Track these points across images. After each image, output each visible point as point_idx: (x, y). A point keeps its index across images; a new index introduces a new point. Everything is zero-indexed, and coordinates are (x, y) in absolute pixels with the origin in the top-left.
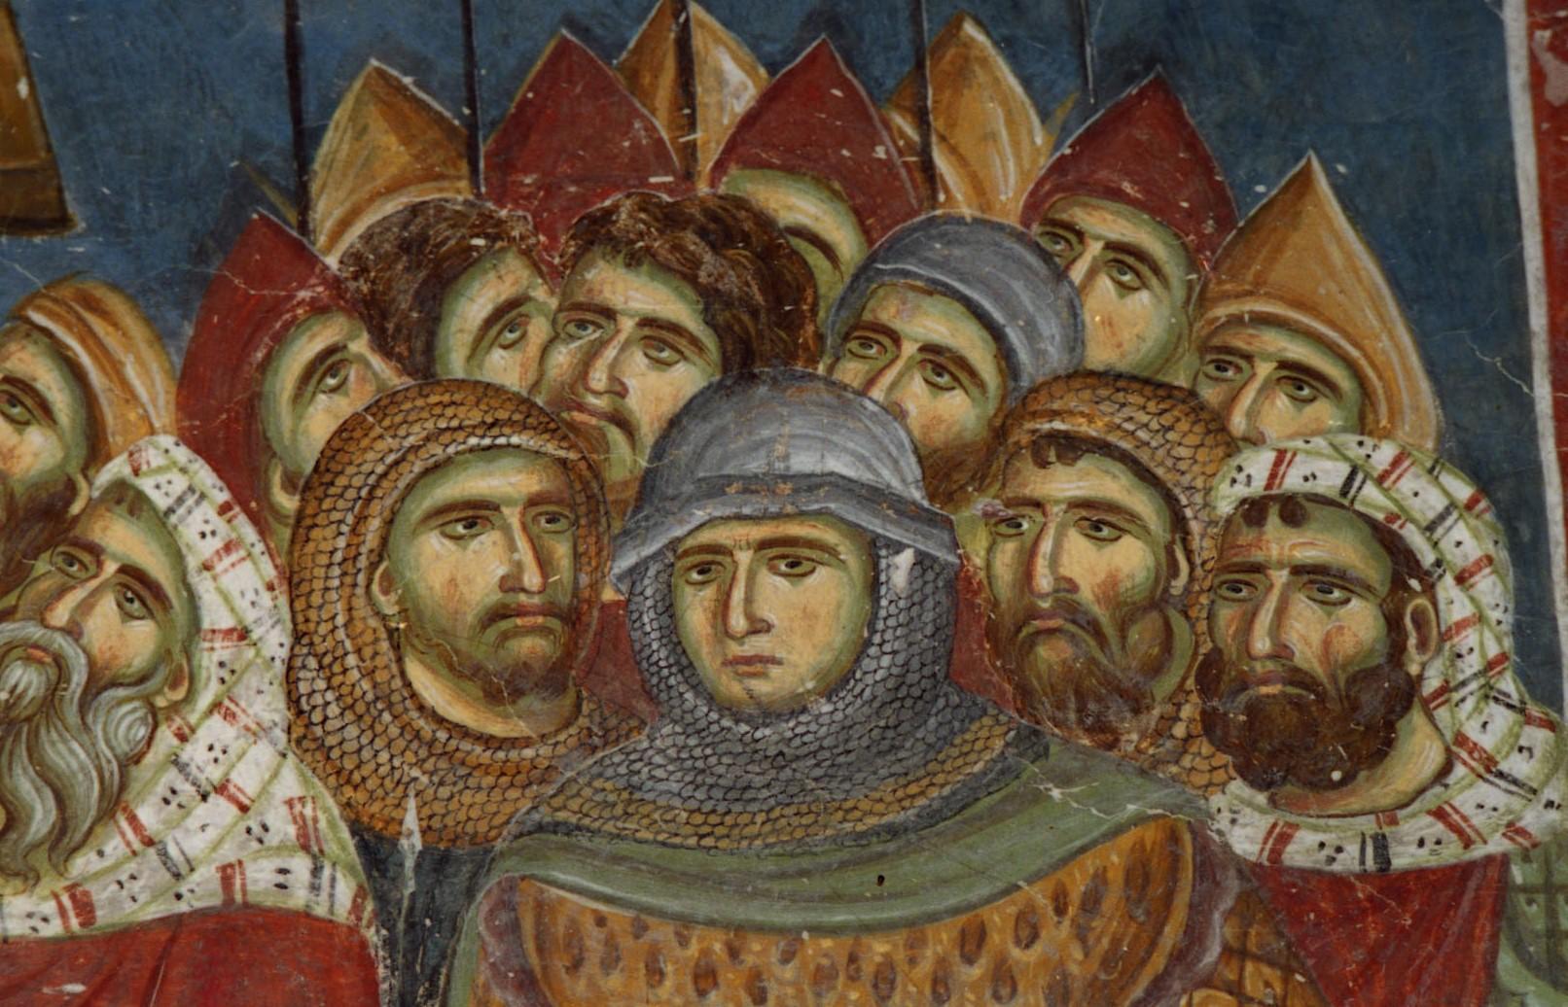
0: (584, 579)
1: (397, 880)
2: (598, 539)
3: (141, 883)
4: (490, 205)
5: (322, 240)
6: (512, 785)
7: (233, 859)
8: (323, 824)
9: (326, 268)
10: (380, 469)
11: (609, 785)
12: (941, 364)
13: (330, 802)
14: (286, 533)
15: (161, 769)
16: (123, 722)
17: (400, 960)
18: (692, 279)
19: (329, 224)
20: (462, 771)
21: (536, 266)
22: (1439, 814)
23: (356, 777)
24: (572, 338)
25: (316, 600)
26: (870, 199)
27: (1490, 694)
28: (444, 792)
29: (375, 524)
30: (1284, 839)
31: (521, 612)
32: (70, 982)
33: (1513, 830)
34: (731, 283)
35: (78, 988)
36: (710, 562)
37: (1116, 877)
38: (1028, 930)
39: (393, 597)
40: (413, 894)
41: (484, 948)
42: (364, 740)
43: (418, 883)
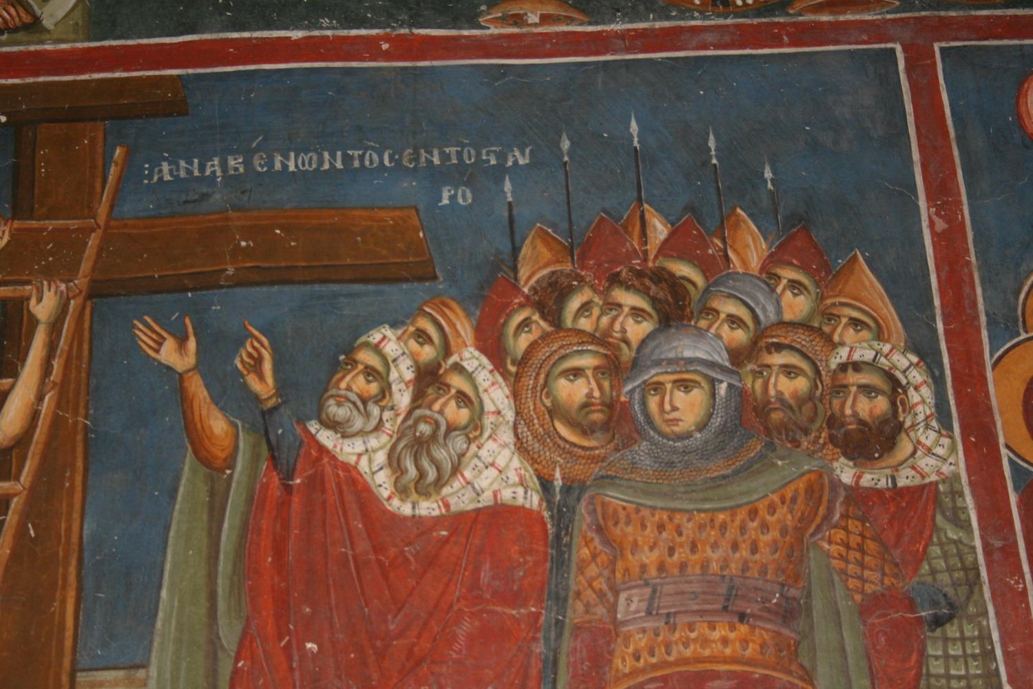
0: (614, 394)
1: (554, 495)
2: (619, 380)
3: (466, 496)
4: (579, 271)
5: (522, 283)
6: (592, 463)
7: (497, 488)
8: (527, 476)
9: (523, 292)
10: (544, 358)
11: (625, 463)
12: (734, 320)
13: (530, 469)
14: (513, 379)
15: (472, 458)
16: (459, 443)
17: (556, 522)
18: (648, 295)
19: (524, 278)
20: (575, 458)
21: (595, 290)
22: (913, 468)
23: (538, 460)
24: (607, 314)
25: (523, 401)
26: (706, 266)
27: (927, 427)
28: (569, 465)
29: (542, 376)
30: (859, 477)
31: (593, 404)
32: (443, 530)
33: (939, 473)
34: (661, 295)
35: (444, 533)
36: (658, 387)
37: (802, 491)
38: (772, 509)
39: (549, 400)
40: (559, 501)
41: (584, 518)
42: (541, 448)
43: (561, 497)
